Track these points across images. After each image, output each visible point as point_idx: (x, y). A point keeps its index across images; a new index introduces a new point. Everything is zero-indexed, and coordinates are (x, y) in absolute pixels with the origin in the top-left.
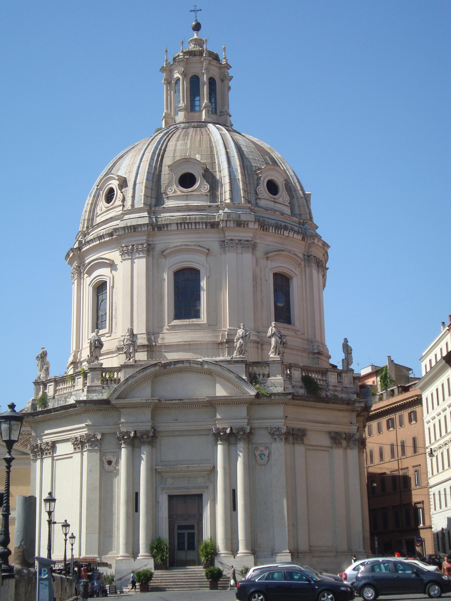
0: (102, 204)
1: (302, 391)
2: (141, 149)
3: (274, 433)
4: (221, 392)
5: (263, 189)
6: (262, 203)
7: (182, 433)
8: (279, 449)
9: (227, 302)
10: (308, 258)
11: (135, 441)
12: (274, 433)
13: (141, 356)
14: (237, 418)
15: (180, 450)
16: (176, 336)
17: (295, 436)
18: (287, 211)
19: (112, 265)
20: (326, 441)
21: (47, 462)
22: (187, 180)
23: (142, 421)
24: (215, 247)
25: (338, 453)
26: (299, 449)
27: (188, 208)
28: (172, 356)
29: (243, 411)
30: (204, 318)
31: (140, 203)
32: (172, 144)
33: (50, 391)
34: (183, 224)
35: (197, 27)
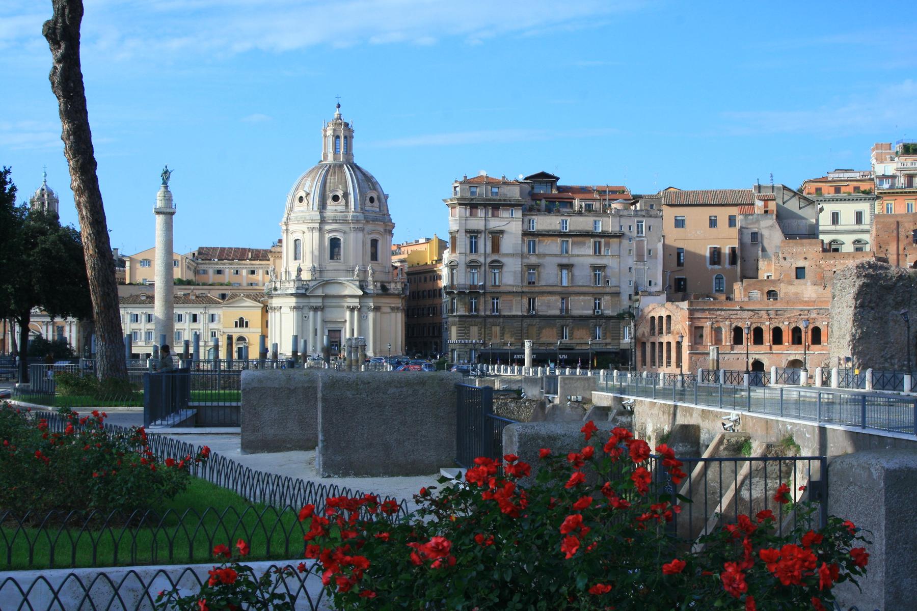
1: (380, 292)
2: (314, 179)
5: (368, 201)
6: (367, 208)
7: (334, 307)
8: (371, 315)
10: (385, 230)
11: (316, 309)
14: (355, 302)
17: (377, 309)
18: (378, 210)
20: (388, 310)
21: (277, 314)
22: (336, 198)
23: (318, 302)
25: (393, 315)
26: (379, 314)
27: (336, 211)
29: (357, 300)
31: (316, 208)
32: (329, 177)
35: (339, 106)
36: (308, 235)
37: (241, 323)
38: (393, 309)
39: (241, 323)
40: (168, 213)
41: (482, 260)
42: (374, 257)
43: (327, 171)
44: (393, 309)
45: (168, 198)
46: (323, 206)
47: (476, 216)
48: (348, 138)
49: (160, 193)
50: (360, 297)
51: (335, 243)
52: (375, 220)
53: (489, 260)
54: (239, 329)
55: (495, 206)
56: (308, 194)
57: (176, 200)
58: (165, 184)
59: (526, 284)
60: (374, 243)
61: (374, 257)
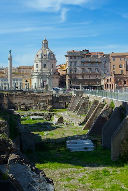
0: (37, 56)
3: (51, 78)
4: (48, 75)
5: (51, 56)
8: (52, 79)
9: (47, 66)
10: (55, 62)
11: (41, 78)
12: (51, 78)
13: (41, 71)
15: (44, 79)
16: (44, 69)
17: (53, 78)
19: (38, 63)
20: (55, 78)
22: (45, 56)
24: (47, 62)
28: (44, 71)
30: (46, 68)
31: (41, 58)
33: (33, 73)
34: (44, 60)
35: (45, 37)
36: (39, 63)
37: (26, 81)
38: (56, 78)
39: (26, 81)
40: (10, 59)
41: (73, 68)
42: (53, 67)
43: (43, 50)
44: (56, 78)
45: (11, 56)
46: (42, 57)
47: (71, 58)
48: (47, 44)
49: (9, 55)
50: (50, 75)
51: (45, 65)
52: (53, 60)
53: (74, 68)
54: (26, 82)
55: (75, 57)
56: (39, 55)
57: (12, 57)
58: (10, 53)
59: (82, 72)
60: (53, 65)
61: (53, 67)
